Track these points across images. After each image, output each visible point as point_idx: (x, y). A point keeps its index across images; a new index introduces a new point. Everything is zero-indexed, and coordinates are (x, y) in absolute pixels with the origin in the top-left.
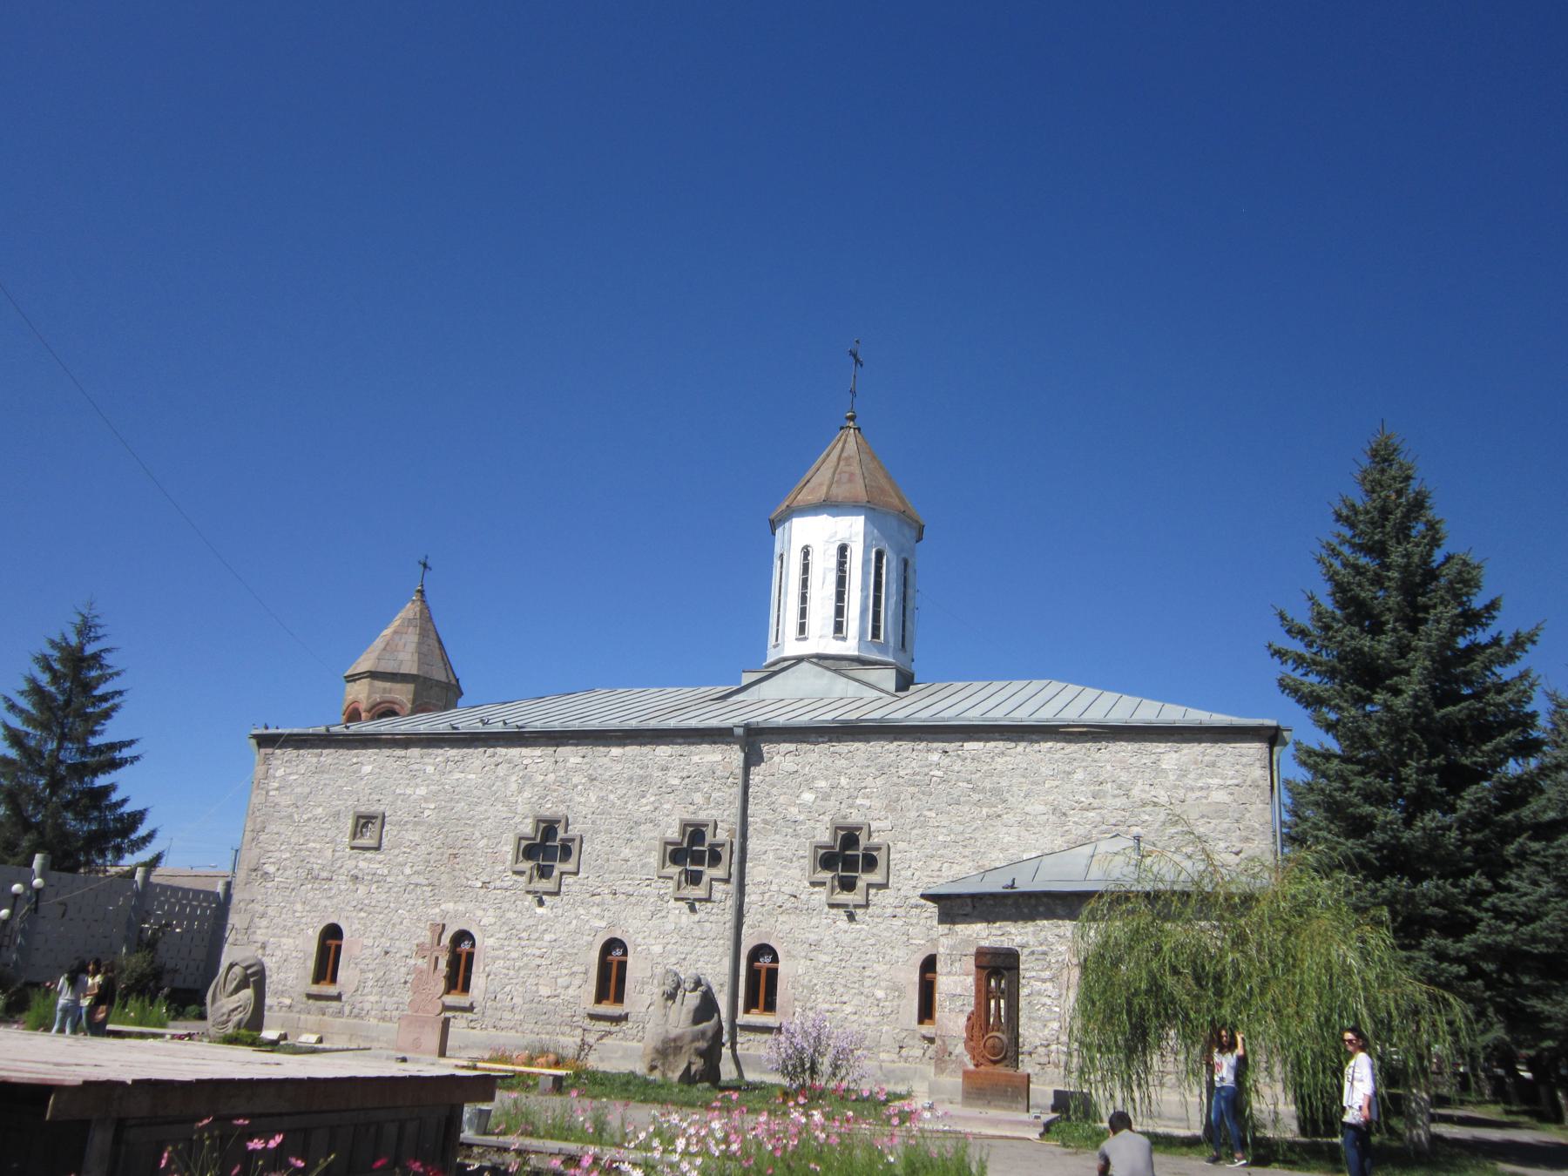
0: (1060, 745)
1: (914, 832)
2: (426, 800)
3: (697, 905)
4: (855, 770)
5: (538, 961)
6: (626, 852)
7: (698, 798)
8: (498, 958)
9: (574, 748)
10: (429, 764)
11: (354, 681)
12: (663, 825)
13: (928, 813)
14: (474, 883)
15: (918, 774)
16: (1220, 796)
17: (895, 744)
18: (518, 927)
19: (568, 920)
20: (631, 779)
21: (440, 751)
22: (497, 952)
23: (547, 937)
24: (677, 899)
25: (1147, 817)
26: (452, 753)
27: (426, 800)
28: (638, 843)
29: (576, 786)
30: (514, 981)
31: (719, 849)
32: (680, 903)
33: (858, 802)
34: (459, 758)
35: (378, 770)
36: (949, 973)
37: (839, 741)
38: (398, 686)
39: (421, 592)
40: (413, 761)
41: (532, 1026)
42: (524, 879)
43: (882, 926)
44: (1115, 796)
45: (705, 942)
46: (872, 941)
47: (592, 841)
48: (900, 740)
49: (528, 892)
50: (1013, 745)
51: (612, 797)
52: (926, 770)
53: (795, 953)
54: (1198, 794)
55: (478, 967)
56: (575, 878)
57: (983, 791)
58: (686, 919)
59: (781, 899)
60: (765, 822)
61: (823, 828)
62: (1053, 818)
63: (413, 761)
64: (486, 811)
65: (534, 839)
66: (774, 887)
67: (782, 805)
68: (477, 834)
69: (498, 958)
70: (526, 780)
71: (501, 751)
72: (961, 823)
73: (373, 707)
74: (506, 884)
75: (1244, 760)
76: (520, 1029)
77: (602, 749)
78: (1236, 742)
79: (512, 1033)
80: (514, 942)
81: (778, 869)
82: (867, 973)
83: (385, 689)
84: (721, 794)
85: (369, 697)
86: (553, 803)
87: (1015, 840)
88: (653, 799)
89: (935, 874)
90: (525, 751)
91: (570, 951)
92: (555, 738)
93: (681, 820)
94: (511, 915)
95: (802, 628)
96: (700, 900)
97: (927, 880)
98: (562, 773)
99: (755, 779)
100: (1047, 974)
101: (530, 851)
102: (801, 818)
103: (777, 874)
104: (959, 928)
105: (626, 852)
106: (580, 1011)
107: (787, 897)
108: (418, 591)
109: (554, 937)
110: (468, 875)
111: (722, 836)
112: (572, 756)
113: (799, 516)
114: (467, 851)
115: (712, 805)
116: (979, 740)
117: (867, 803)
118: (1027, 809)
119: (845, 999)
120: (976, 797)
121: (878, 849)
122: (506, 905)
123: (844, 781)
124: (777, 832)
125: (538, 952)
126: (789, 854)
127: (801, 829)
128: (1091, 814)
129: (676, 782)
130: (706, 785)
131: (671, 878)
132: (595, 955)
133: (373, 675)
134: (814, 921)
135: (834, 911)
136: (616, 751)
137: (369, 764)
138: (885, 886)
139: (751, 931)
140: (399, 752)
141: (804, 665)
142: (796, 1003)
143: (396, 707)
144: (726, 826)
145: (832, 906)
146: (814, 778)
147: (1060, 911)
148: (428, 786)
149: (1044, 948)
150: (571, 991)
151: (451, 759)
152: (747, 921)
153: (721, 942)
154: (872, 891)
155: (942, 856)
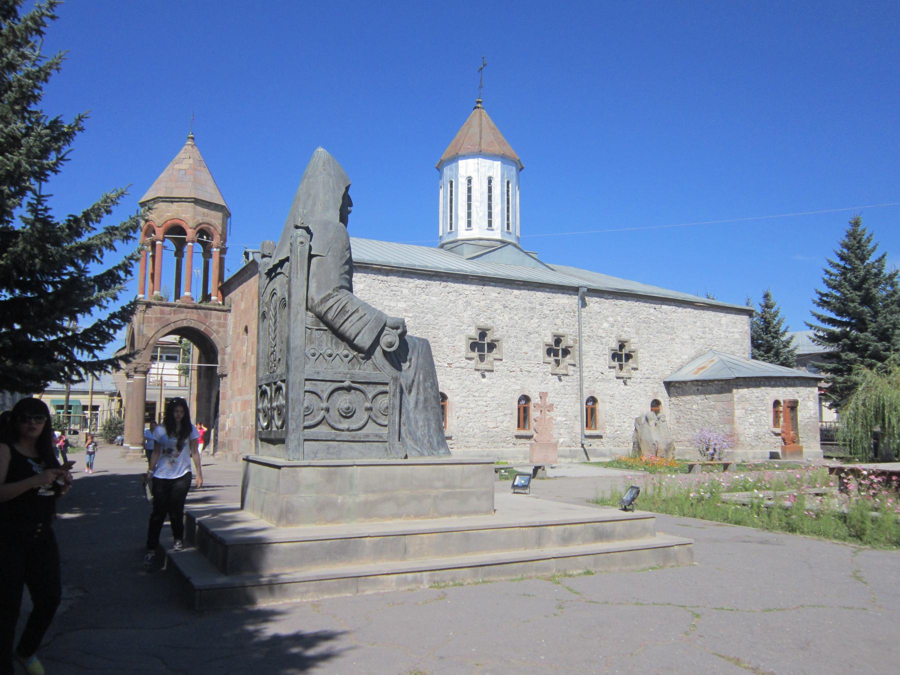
0: (693, 310)
1: (646, 344)
2: (406, 311)
3: (562, 378)
4: (623, 314)
5: (486, 409)
6: (525, 348)
7: (558, 322)
8: (462, 408)
9: (493, 288)
10: (405, 288)
11: (172, 202)
12: (543, 335)
13: (650, 336)
14: (443, 363)
15: (646, 318)
16: (737, 336)
17: (638, 303)
18: (472, 390)
19: (499, 386)
20: (525, 308)
21: (411, 280)
22: (461, 405)
23: (489, 395)
24: (552, 374)
25: (717, 343)
26: (421, 281)
27: (406, 311)
28: (531, 344)
29: (496, 310)
30: (474, 420)
31: (569, 349)
32: (554, 376)
33: (626, 329)
34: (424, 286)
35: (368, 288)
36: (738, 409)
37: (617, 299)
38: (213, 213)
39: (193, 138)
40: (392, 284)
41: (486, 444)
42: (473, 362)
43: (636, 387)
44: (709, 333)
45: (567, 396)
46: (634, 394)
47: (508, 342)
48: (640, 301)
49: (476, 370)
50: (677, 308)
51: (516, 318)
52: (649, 316)
53: (605, 400)
54: (732, 334)
55: (452, 414)
56: (501, 362)
57: (668, 328)
58: (558, 384)
59: (597, 375)
60: (589, 336)
61: (612, 340)
62: (690, 341)
63: (392, 284)
64: (445, 320)
65: (476, 339)
66: (594, 369)
67: (595, 328)
68: (441, 334)
69: (462, 408)
70: (468, 303)
71: (452, 285)
72: (662, 341)
73: (197, 227)
74: (463, 365)
75: (744, 322)
76: (480, 446)
77: (509, 290)
78: (740, 315)
79: (476, 449)
80: (471, 398)
81: (596, 360)
82: (632, 408)
83: (204, 214)
84: (568, 320)
85: (194, 218)
86: (485, 319)
87: (679, 349)
88: (537, 320)
89: (654, 364)
90: (464, 286)
91: (502, 402)
92: (482, 281)
93: (553, 333)
94: (467, 383)
95: (490, 224)
96: (563, 375)
97: (651, 366)
98: (488, 301)
99: (584, 314)
100: (764, 408)
101: (474, 346)
102: (604, 335)
103: (595, 362)
104: (740, 390)
105: (525, 348)
106: (510, 434)
107: (600, 373)
108: (193, 138)
109: (493, 395)
110: (440, 360)
111: (570, 343)
112: (492, 292)
113: (482, 158)
114: (436, 344)
115: (565, 326)
116: (667, 305)
117: (628, 329)
118: (683, 337)
119: (625, 420)
120: (667, 330)
121: (634, 352)
122: (463, 377)
123: (619, 319)
124: (594, 342)
125: (485, 404)
126: (599, 353)
127: (604, 340)
128: (702, 340)
129: (548, 312)
130: (562, 315)
131: (550, 363)
132: (515, 405)
133: (197, 201)
134: (611, 385)
135: (619, 380)
136: (516, 292)
137: (361, 283)
138: (636, 369)
139: (586, 390)
140: (381, 277)
141: (510, 246)
142: (607, 424)
143: (184, 225)
144: (572, 337)
145: (618, 378)
146: (608, 316)
147: (767, 384)
148: (405, 302)
149: (763, 398)
150: (505, 424)
151: (419, 286)
152: (585, 385)
153: (574, 396)
154: (633, 371)
155: (656, 356)
